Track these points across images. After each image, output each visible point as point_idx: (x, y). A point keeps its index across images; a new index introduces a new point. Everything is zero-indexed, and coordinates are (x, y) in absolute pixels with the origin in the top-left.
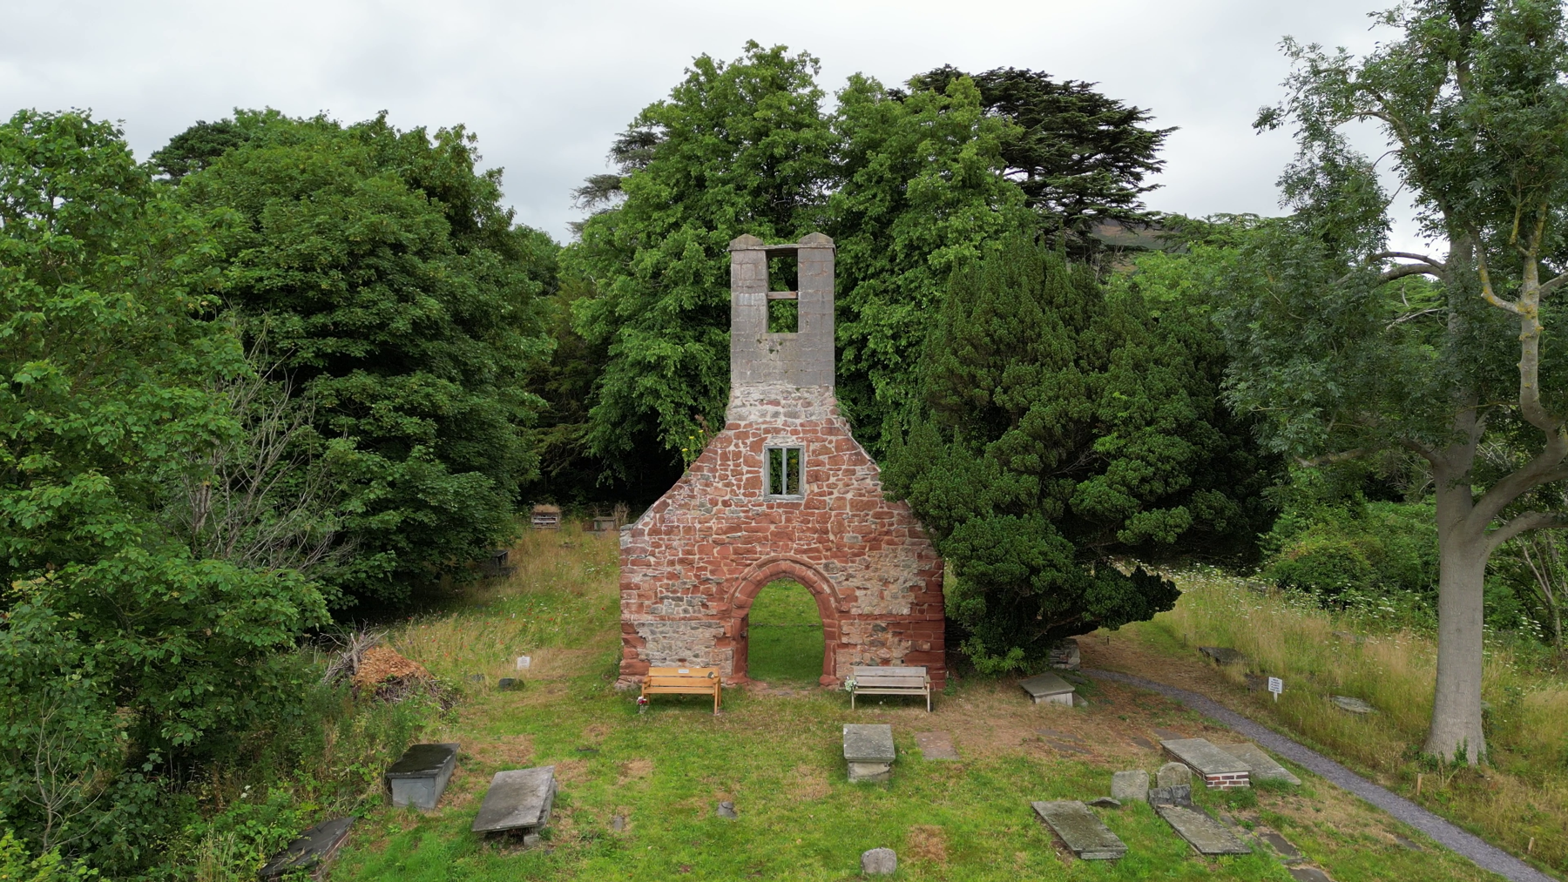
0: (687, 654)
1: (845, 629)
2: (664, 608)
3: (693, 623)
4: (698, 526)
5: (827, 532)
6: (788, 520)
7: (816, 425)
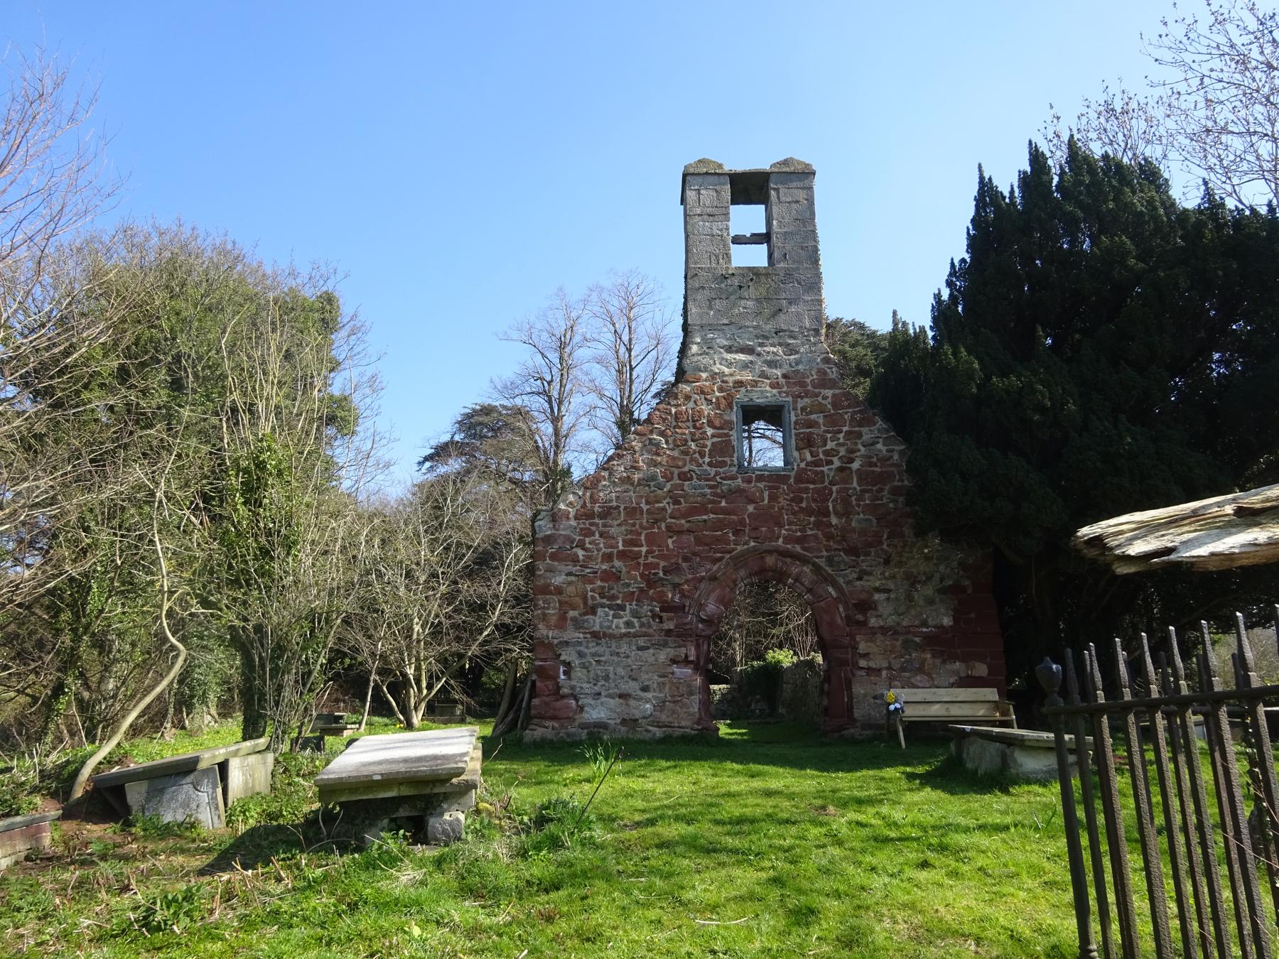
0: (632, 687)
1: (863, 647)
2: (597, 622)
3: (641, 642)
4: (645, 507)
5: (827, 514)
6: (773, 498)
7: (804, 376)
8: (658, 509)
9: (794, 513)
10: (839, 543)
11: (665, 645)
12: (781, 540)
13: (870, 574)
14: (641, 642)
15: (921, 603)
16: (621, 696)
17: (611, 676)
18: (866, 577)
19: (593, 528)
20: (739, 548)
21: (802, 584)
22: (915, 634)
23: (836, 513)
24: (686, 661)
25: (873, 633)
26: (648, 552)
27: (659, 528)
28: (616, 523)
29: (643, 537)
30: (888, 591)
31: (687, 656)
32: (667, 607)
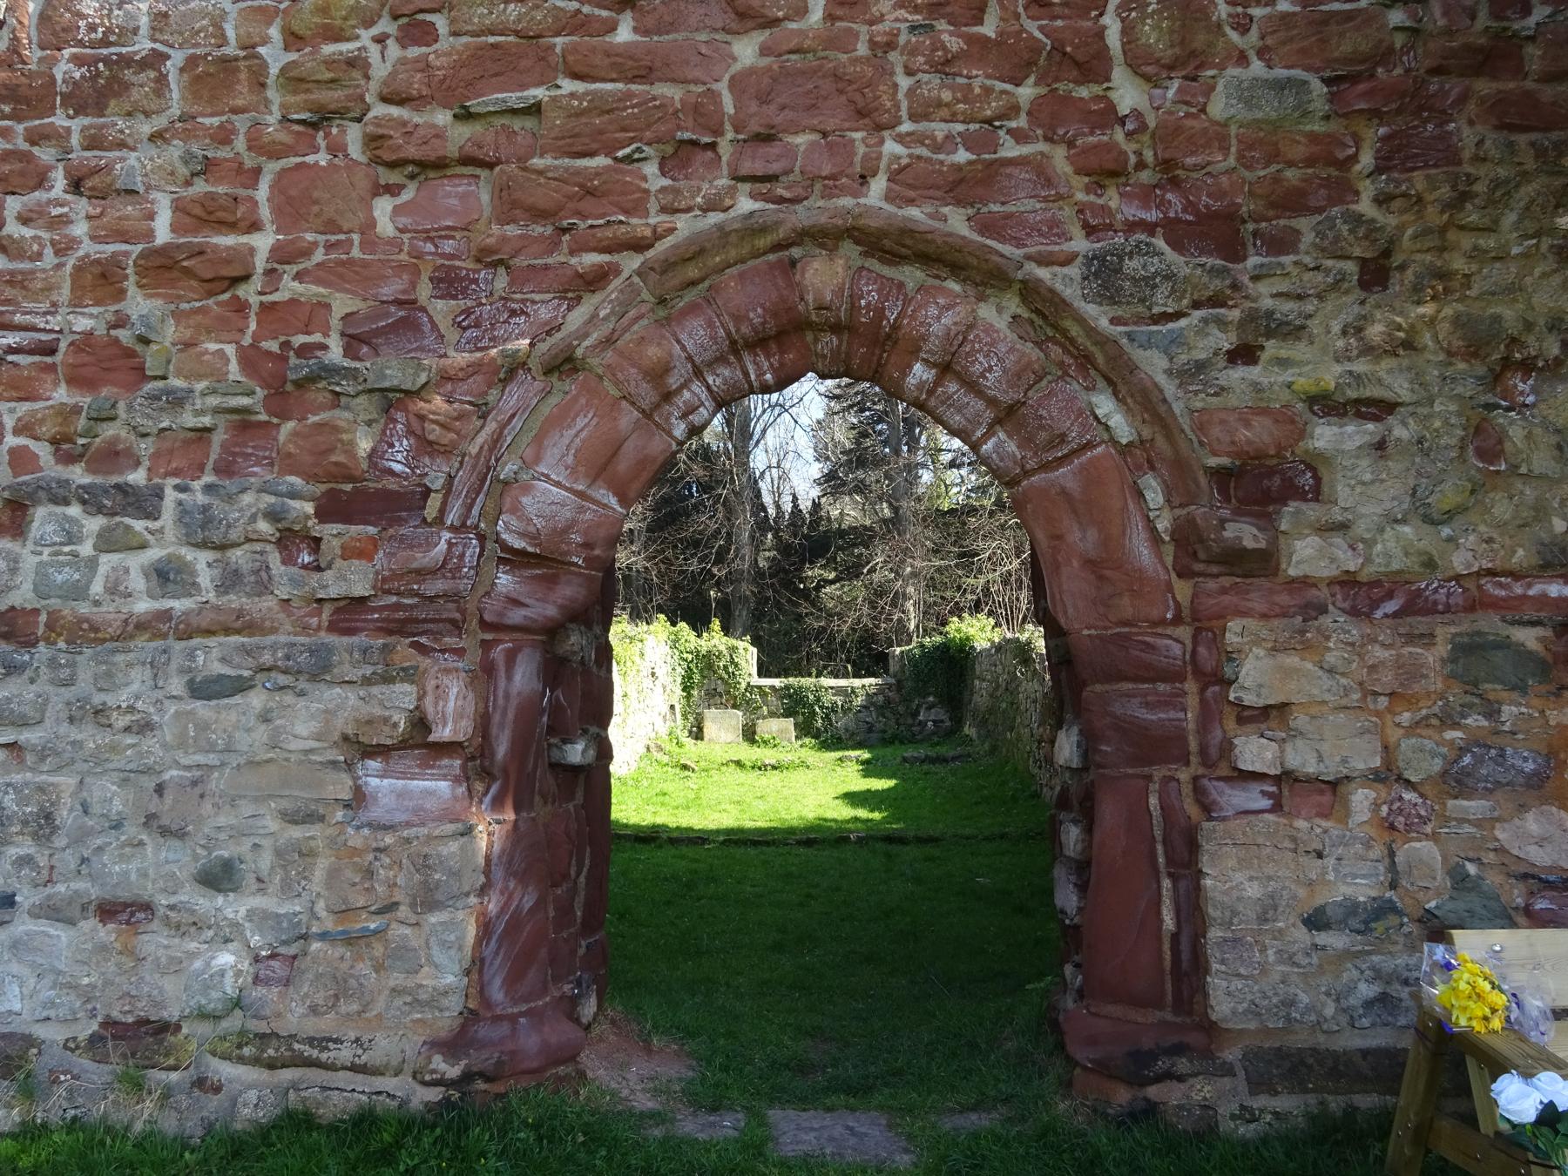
0: (151, 868)
1: (1256, 676)
3: (211, 657)
4: (274, 56)
5: (1093, 66)
8: (330, 63)
9: (944, 65)
10: (1146, 196)
11: (320, 670)
12: (878, 185)
13: (1292, 331)
14: (211, 657)
15: (1542, 461)
16: (108, 911)
17: (66, 815)
18: (1272, 348)
19: (45, 154)
20: (685, 225)
21: (972, 386)
22: (1511, 609)
23: (1138, 62)
24: (418, 743)
25: (1305, 604)
26: (283, 255)
27: (336, 149)
28: (146, 129)
29: (262, 192)
30: (1381, 409)
31: (420, 724)
32: (356, 500)
